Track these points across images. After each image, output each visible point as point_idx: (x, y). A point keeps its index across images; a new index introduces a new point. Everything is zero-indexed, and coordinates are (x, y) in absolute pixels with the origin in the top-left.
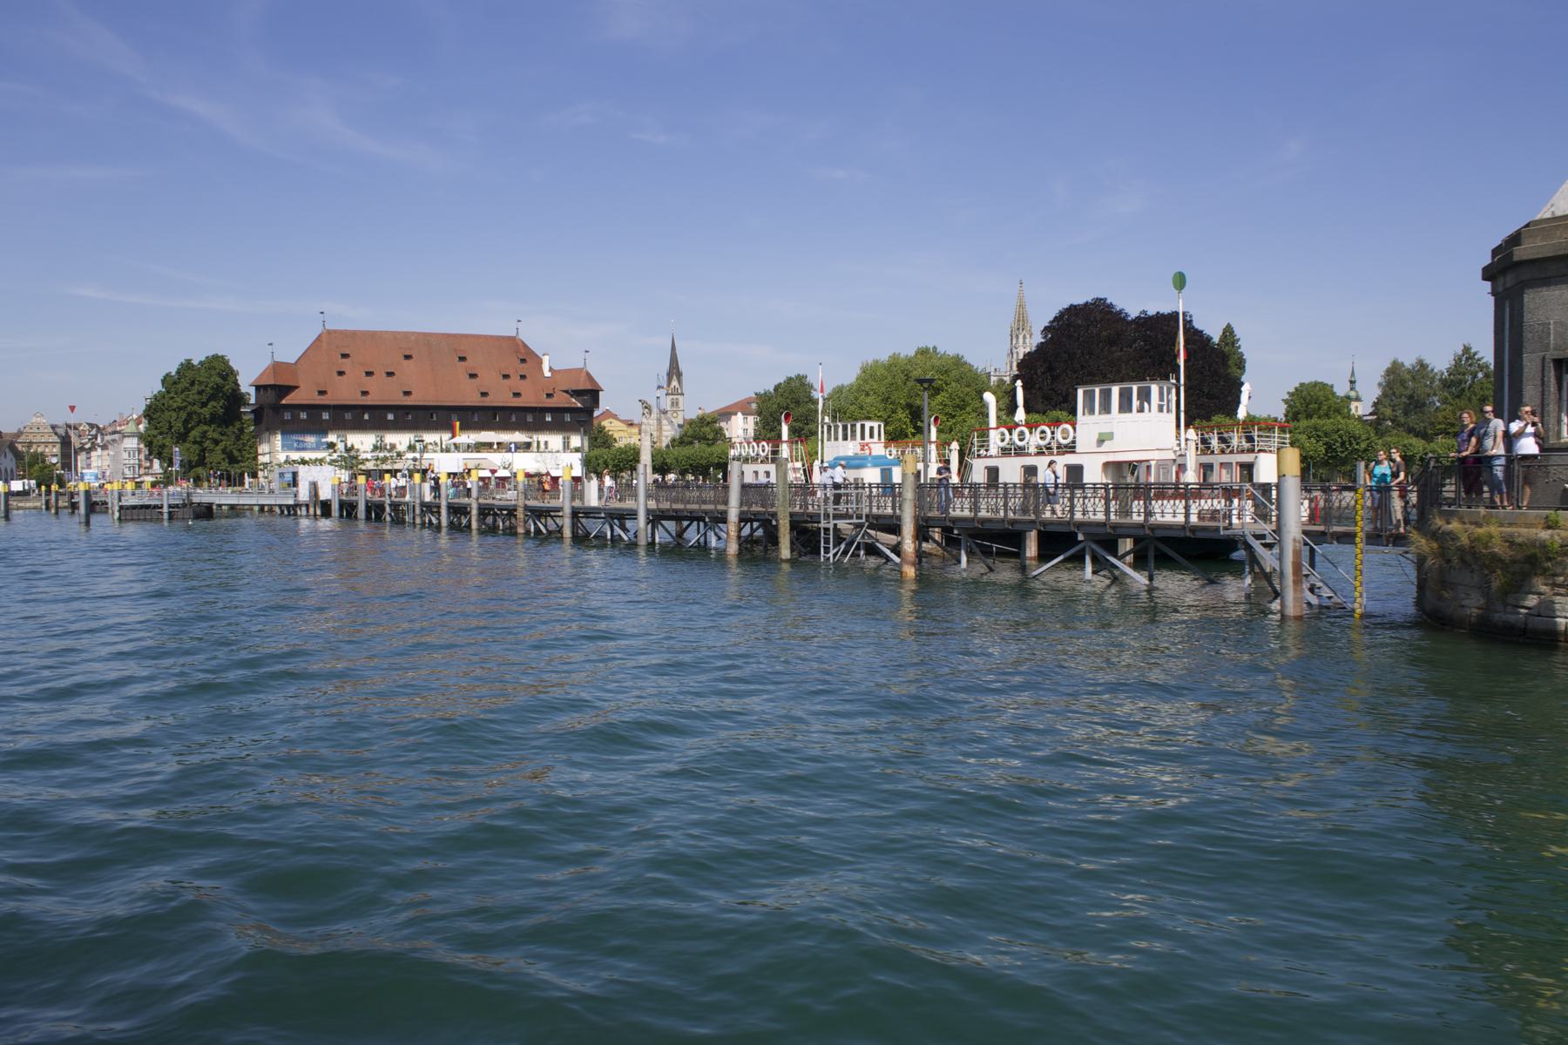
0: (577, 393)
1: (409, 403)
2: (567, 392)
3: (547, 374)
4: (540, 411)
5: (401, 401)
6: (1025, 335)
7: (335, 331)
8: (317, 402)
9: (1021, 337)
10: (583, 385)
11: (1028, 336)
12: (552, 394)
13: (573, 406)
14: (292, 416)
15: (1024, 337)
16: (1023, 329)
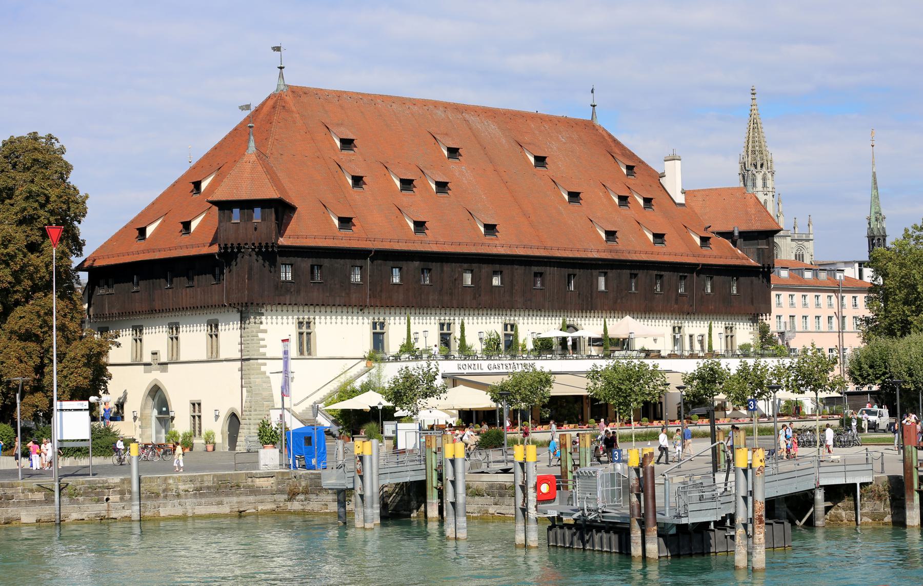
0: (749, 236)
2: (714, 233)
3: (680, 199)
5: (482, 244)
6: (765, 174)
7: (305, 92)
9: (759, 177)
11: (769, 175)
15: (764, 179)
16: (762, 165)
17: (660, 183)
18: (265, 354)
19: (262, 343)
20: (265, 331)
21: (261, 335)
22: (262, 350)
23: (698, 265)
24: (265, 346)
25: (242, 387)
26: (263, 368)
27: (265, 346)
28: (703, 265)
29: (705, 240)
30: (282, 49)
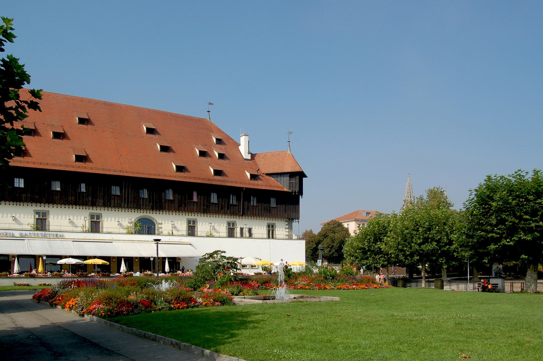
12: (257, 176)
23: (243, 188)
28: (246, 188)
29: (253, 177)
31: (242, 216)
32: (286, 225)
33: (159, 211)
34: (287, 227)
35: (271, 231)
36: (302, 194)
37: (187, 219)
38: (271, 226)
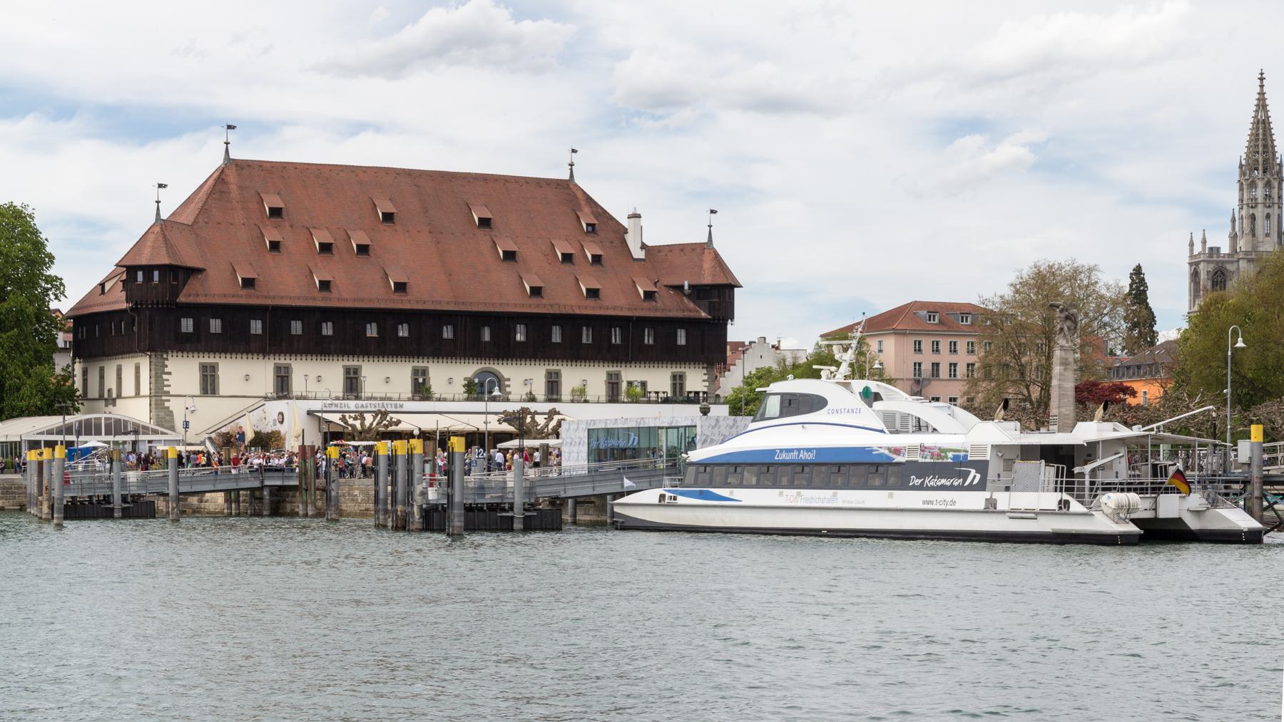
0: (699, 292)
1: (407, 306)
4: (631, 325)
8: (243, 301)
10: (708, 277)
13: (692, 315)
14: (196, 325)
17: (624, 239)
18: (169, 392)
19: (166, 383)
20: (170, 373)
21: (165, 377)
22: (166, 389)
23: (632, 317)
24: (169, 386)
25: (150, 419)
26: (167, 404)
27: (169, 386)
30: (226, 127)
31: (631, 363)
32: (705, 374)
33: (507, 360)
34: (706, 377)
35: (678, 385)
36: (732, 319)
37: (413, 367)
38: (678, 377)
